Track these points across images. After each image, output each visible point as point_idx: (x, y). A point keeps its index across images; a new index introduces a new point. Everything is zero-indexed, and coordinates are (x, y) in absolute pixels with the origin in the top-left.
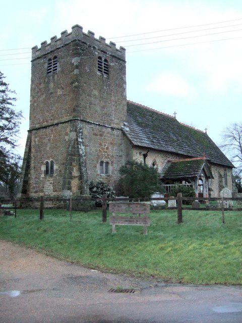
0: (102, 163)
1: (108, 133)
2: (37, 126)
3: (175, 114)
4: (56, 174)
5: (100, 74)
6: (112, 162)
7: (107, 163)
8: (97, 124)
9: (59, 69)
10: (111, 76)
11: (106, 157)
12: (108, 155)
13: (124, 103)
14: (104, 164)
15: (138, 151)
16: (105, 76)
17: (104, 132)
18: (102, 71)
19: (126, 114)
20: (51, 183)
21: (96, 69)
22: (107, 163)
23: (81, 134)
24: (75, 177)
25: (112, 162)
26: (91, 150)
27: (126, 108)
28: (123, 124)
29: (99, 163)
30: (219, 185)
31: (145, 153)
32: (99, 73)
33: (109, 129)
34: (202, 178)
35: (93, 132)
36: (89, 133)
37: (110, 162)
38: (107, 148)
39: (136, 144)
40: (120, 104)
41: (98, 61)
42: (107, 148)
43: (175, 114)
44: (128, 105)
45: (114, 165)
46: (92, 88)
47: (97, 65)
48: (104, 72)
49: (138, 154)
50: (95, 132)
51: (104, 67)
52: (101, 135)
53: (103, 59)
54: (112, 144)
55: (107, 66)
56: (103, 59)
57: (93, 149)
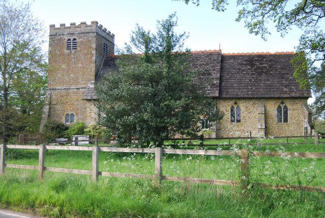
1: (74, 93)
10: (78, 49)
16: (73, 51)
32: (68, 51)
33: (75, 90)
37: (75, 114)
55: (75, 43)
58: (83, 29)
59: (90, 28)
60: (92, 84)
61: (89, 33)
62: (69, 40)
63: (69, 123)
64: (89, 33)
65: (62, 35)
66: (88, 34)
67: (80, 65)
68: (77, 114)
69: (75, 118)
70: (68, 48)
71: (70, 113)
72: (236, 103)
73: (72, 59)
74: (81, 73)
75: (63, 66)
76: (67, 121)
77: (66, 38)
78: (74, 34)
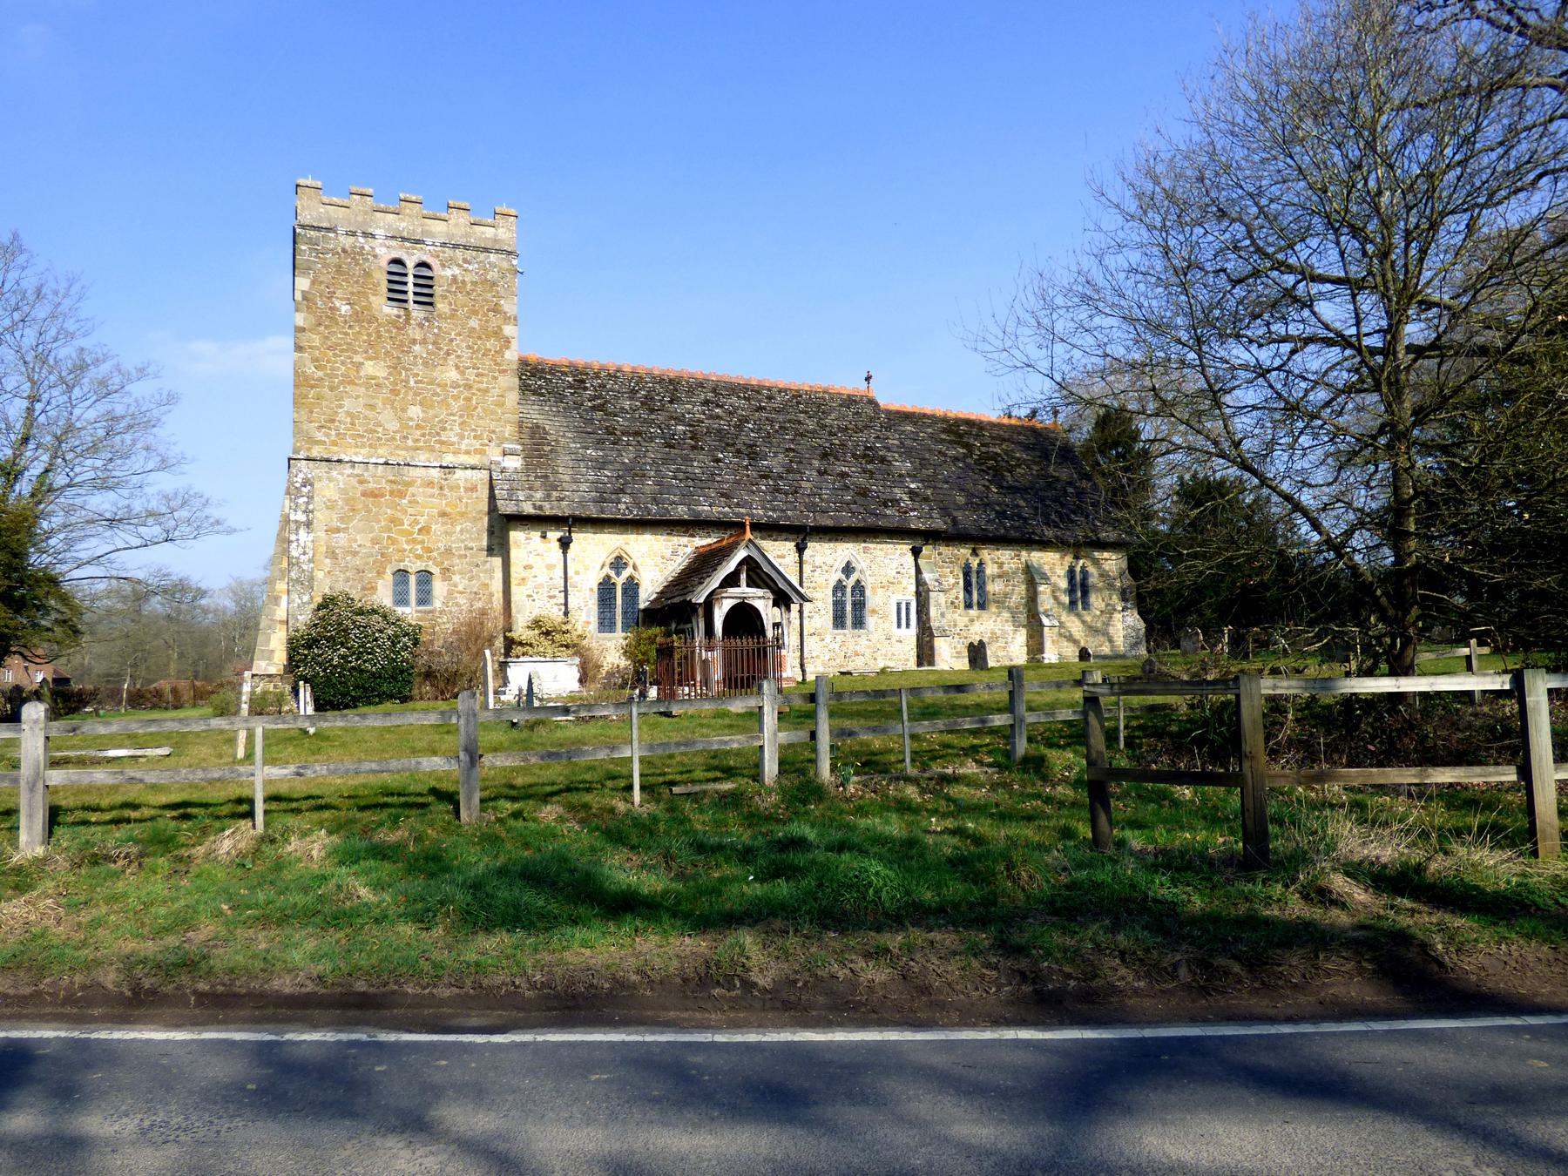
0: (402, 574)
1: (430, 484)
5: (395, 311)
7: (425, 577)
10: (441, 306)
11: (419, 557)
16: (418, 313)
17: (410, 484)
18: (406, 301)
23: (302, 500)
28: (500, 449)
30: (1029, 611)
32: (391, 310)
33: (435, 474)
36: (344, 491)
45: (456, 578)
46: (357, 358)
47: (384, 285)
50: (371, 485)
52: (402, 495)
53: (410, 264)
55: (425, 283)
61: (486, 250)
63: (407, 610)
64: (486, 250)
65: (365, 234)
66: (483, 256)
67: (453, 375)
68: (446, 572)
69: (439, 588)
70: (396, 295)
71: (414, 566)
73: (414, 342)
74: (456, 406)
75: (370, 368)
76: (401, 599)
78: (423, 242)
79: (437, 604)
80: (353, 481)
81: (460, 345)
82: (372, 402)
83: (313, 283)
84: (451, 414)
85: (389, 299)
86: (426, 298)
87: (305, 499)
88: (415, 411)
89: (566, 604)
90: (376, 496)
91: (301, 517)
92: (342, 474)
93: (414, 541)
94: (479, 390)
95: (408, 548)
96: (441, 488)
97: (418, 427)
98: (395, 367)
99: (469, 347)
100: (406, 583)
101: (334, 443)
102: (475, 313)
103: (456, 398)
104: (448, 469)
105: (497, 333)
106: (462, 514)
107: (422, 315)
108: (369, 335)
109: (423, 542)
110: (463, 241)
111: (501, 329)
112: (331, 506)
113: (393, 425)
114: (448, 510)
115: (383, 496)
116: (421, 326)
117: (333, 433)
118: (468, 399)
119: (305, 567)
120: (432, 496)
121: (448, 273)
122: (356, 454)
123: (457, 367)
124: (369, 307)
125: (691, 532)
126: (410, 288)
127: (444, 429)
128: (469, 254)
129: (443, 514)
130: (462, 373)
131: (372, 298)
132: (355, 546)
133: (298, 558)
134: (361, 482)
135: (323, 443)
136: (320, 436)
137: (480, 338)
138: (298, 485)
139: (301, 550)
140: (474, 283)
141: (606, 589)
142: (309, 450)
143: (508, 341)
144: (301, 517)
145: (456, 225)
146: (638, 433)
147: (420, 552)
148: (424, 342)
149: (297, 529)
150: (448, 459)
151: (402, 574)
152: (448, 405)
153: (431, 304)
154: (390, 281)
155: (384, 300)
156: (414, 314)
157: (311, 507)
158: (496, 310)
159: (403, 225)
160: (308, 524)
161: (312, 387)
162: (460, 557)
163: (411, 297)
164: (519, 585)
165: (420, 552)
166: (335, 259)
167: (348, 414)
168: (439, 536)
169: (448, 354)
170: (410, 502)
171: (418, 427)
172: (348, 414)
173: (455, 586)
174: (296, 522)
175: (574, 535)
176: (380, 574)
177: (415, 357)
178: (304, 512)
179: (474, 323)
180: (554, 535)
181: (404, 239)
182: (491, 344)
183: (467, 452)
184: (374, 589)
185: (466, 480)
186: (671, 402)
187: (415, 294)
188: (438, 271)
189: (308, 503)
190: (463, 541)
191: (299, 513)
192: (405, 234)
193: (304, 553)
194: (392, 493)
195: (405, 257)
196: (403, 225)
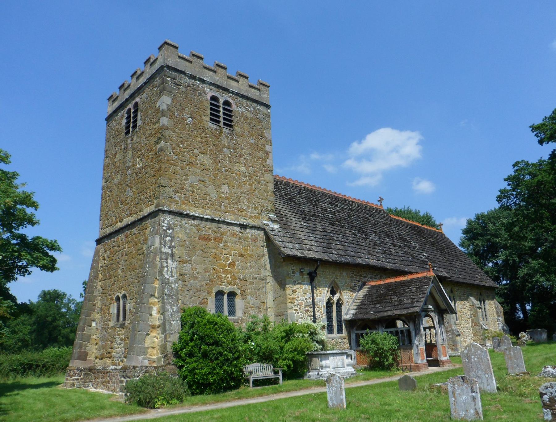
0: (220, 294)
1: (234, 235)
2: (108, 231)
3: (381, 200)
4: (129, 322)
5: (215, 126)
6: (243, 292)
7: (232, 295)
8: (207, 220)
9: (139, 123)
11: (230, 283)
12: (234, 278)
13: (268, 177)
14: (225, 297)
15: (297, 268)
16: (226, 130)
19: (272, 198)
20: (122, 340)
21: (207, 118)
22: (232, 295)
23: (168, 238)
24: (153, 327)
25: (243, 292)
26: (194, 269)
27: (271, 187)
28: (267, 217)
29: (213, 295)
31: (312, 269)
33: (237, 229)
34: (432, 314)
35: (198, 234)
36: (188, 235)
37: (238, 292)
38: (232, 265)
39: (290, 253)
40: (258, 182)
41: (211, 104)
42: (232, 265)
43: (381, 200)
44: (275, 181)
45: (249, 297)
46: (196, 151)
47: (209, 112)
48: (224, 124)
49: (297, 274)
50: (204, 233)
51: (219, 112)
53: (221, 101)
54: (241, 255)
55: (228, 114)
56: (221, 101)
57: (199, 268)
58: (241, 87)
59: (257, 92)
60: (274, 221)
62: (214, 98)
66: (255, 105)
67: (243, 169)
69: (239, 302)
70: (215, 118)
71: (227, 289)
72: (452, 292)
74: (245, 188)
75: (202, 158)
77: (210, 92)
79: (239, 313)
80: (194, 229)
81: (246, 150)
82: (203, 180)
83: (173, 101)
84: (243, 193)
85: (212, 119)
86: (229, 124)
87: (168, 238)
88: (225, 188)
89: (314, 315)
90: (206, 240)
91: (168, 251)
92: (188, 224)
93: (226, 272)
94: (256, 180)
95: (224, 276)
96: (240, 238)
97: (227, 198)
98: (216, 160)
99: (250, 154)
100: (222, 300)
101: (184, 204)
102: (253, 135)
103: (245, 183)
104: (243, 227)
105: (263, 149)
106: (251, 256)
107: (228, 131)
108: (202, 138)
109: (231, 273)
110: (245, 94)
111: (265, 147)
112: (182, 244)
113: (214, 195)
114: (243, 252)
115: (210, 240)
116: (228, 138)
117: (183, 196)
118: (251, 185)
119: (173, 286)
120: (235, 243)
121: (240, 110)
122: (194, 211)
123: (245, 165)
124: (201, 121)
125: (360, 273)
126: (221, 113)
127: (240, 201)
128: (249, 103)
129: (241, 255)
130: (248, 169)
131: (204, 117)
132: (195, 273)
133: (168, 279)
134: (198, 230)
135: (177, 202)
136: (175, 196)
137: (255, 150)
138: (165, 228)
139: (169, 274)
140: (252, 119)
141: (329, 305)
142: (170, 205)
143: (267, 153)
144: (168, 251)
145: (242, 85)
146: (315, 216)
147: (230, 279)
148: (229, 148)
149: (166, 259)
150: (242, 221)
151: (220, 294)
152: (241, 187)
153: (231, 126)
154: (212, 109)
155: (209, 119)
156: (224, 130)
157: (173, 244)
158: (262, 136)
159: (218, 78)
160: (172, 255)
161: (172, 165)
162: (251, 283)
163: (221, 119)
164: (291, 302)
165: (230, 279)
166: (184, 89)
167: (191, 185)
168: (240, 270)
169: (240, 156)
170: (224, 245)
171: (227, 198)
172: (191, 185)
173: (249, 303)
174: (166, 253)
175: (318, 271)
176: (209, 293)
177: (225, 155)
178: (170, 247)
179: (252, 141)
180: (307, 270)
181: (219, 87)
182: (260, 154)
183: (251, 217)
184: (206, 303)
185: (252, 235)
186: (318, 201)
187: (224, 119)
188: (234, 108)
189: (171, 241)
190: (251, 273)
191: (167, 247)
192: (219, 84)
193: (172, 276)
194: (215, 238)
195: (219, 96)
196: (218, 78)
